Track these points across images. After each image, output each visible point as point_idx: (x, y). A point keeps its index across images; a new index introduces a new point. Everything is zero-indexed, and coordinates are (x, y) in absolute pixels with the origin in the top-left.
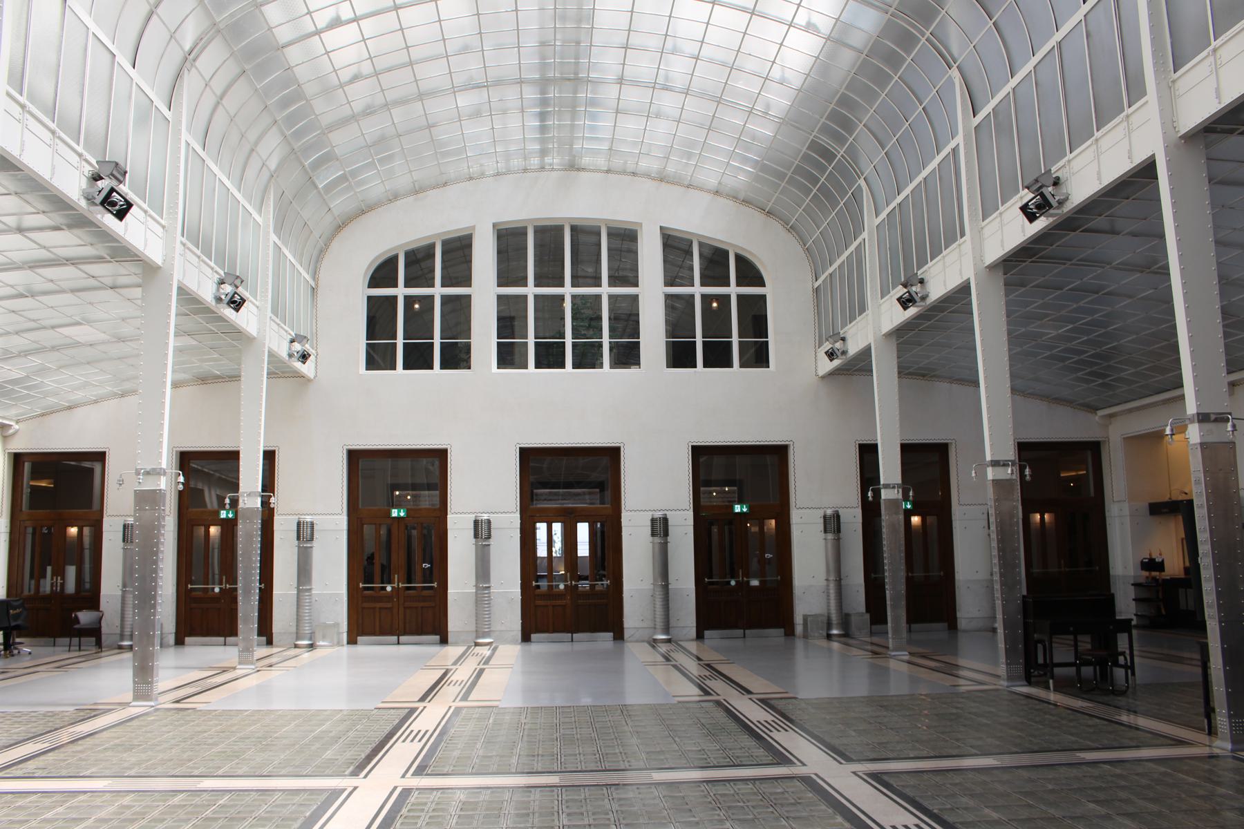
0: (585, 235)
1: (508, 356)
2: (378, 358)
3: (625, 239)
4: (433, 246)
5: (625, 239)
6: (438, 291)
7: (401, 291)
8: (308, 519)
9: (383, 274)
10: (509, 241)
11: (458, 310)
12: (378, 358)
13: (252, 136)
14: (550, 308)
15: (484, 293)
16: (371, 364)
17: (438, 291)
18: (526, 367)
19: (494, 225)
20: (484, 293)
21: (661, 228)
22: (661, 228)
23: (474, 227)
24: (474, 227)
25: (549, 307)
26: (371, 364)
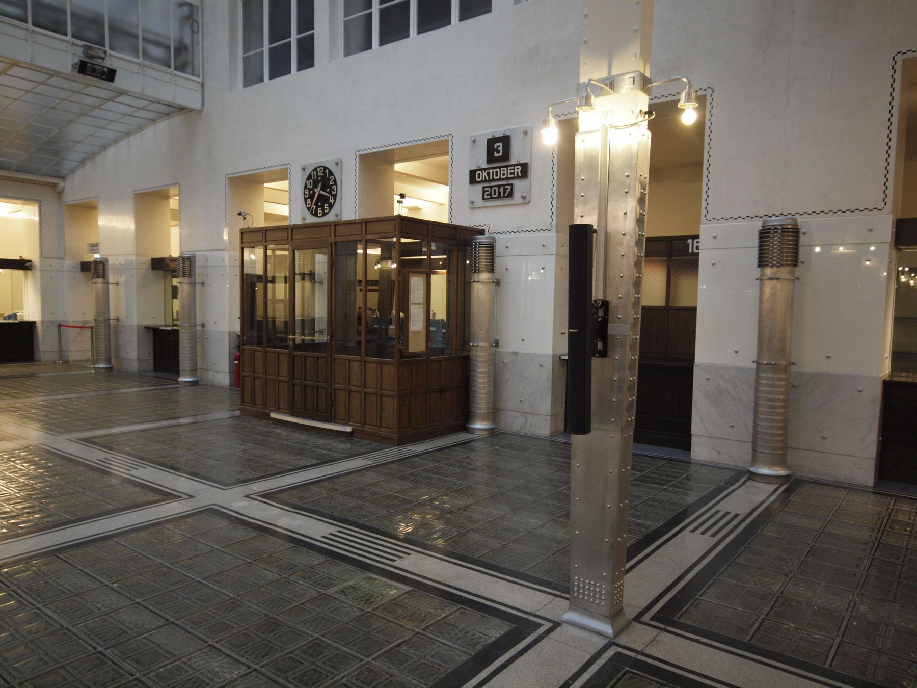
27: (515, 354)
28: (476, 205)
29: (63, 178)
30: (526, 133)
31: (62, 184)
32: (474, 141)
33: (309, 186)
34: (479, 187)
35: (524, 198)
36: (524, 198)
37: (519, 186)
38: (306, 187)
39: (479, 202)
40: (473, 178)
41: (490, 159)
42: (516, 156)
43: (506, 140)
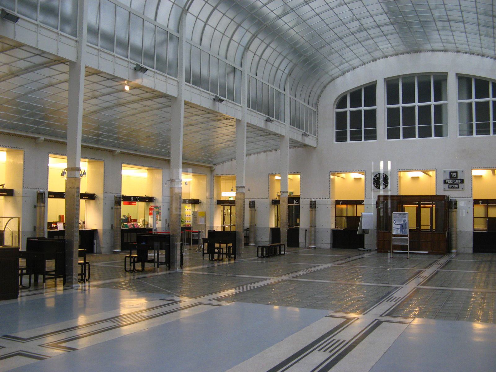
0: (424, 80)
1: (393, 134)
2: (341, 137)
3: (441, 80)
4: (360, 90)
5: (441, 80)
6: (363, 108)
7: (349, 109)
8: (313, 200)
9: (341, 103)
10: (392, 85)
11: (371, 116)
12: (341, 137)
13: (276, 65)
14: (408, 112)
15: (381, 107)
16: (338, 140)
17: (363, 108)
18: (399, 138)
19: (385, 79)
20: (381, 107)
21: (457, 74)
22: (457, 74)
23: (376, 81)
24: (376, 81)
25: (408, 112)
26: (338, 140)
27: (461, 231)
28: (446, 189)
29: (215, 165)
30: (462, 171)
31: (214, 167)
32: (445, 172)
33: (375, 179)
34: (447, 185)
35: (463, 189)
36: (463, 189)
37: (460, 185)
38: (374, 179)
39: (447, 188)
40: (445, 182)
41: (451, 177)
42: (460, 177)
43: (456, 173)
